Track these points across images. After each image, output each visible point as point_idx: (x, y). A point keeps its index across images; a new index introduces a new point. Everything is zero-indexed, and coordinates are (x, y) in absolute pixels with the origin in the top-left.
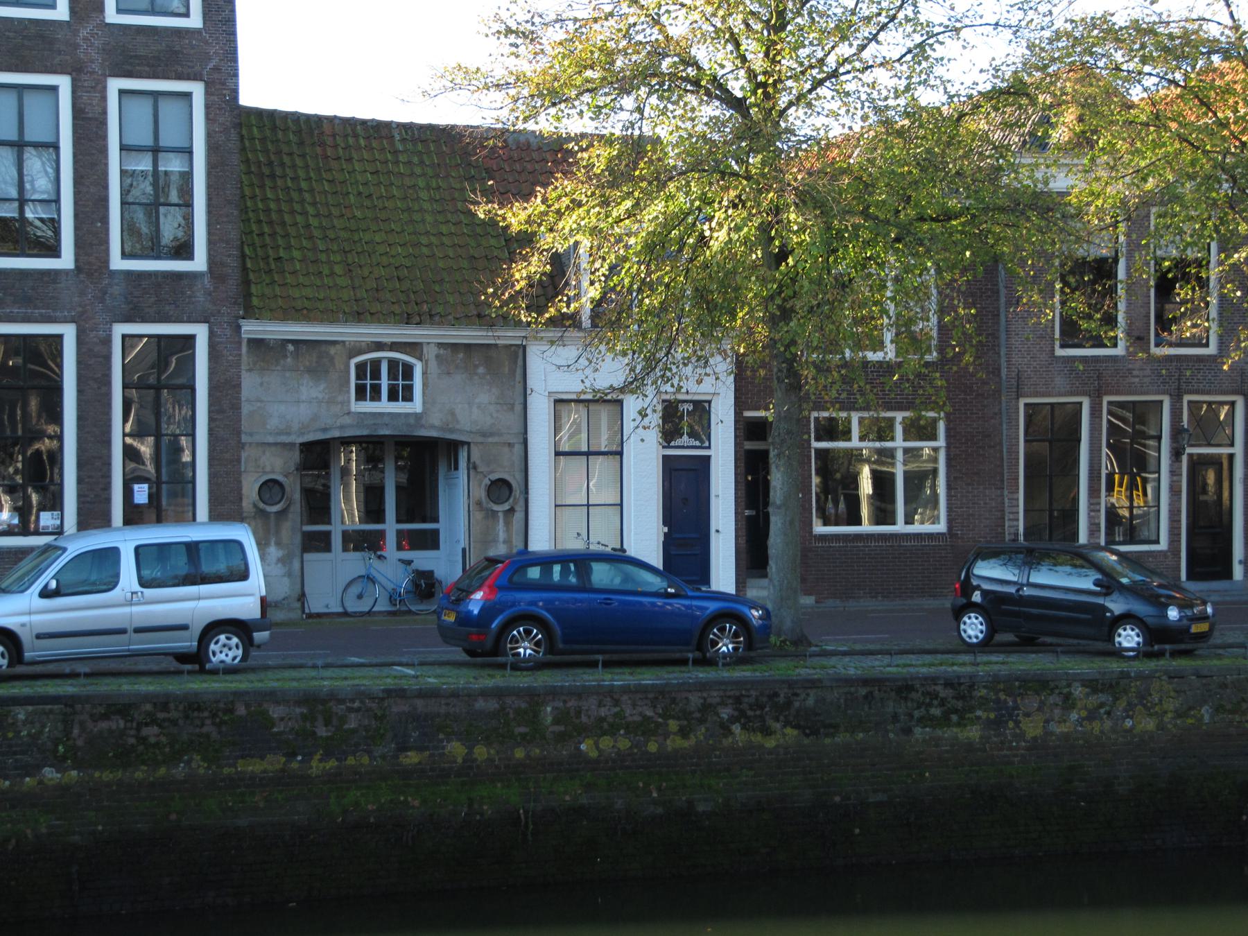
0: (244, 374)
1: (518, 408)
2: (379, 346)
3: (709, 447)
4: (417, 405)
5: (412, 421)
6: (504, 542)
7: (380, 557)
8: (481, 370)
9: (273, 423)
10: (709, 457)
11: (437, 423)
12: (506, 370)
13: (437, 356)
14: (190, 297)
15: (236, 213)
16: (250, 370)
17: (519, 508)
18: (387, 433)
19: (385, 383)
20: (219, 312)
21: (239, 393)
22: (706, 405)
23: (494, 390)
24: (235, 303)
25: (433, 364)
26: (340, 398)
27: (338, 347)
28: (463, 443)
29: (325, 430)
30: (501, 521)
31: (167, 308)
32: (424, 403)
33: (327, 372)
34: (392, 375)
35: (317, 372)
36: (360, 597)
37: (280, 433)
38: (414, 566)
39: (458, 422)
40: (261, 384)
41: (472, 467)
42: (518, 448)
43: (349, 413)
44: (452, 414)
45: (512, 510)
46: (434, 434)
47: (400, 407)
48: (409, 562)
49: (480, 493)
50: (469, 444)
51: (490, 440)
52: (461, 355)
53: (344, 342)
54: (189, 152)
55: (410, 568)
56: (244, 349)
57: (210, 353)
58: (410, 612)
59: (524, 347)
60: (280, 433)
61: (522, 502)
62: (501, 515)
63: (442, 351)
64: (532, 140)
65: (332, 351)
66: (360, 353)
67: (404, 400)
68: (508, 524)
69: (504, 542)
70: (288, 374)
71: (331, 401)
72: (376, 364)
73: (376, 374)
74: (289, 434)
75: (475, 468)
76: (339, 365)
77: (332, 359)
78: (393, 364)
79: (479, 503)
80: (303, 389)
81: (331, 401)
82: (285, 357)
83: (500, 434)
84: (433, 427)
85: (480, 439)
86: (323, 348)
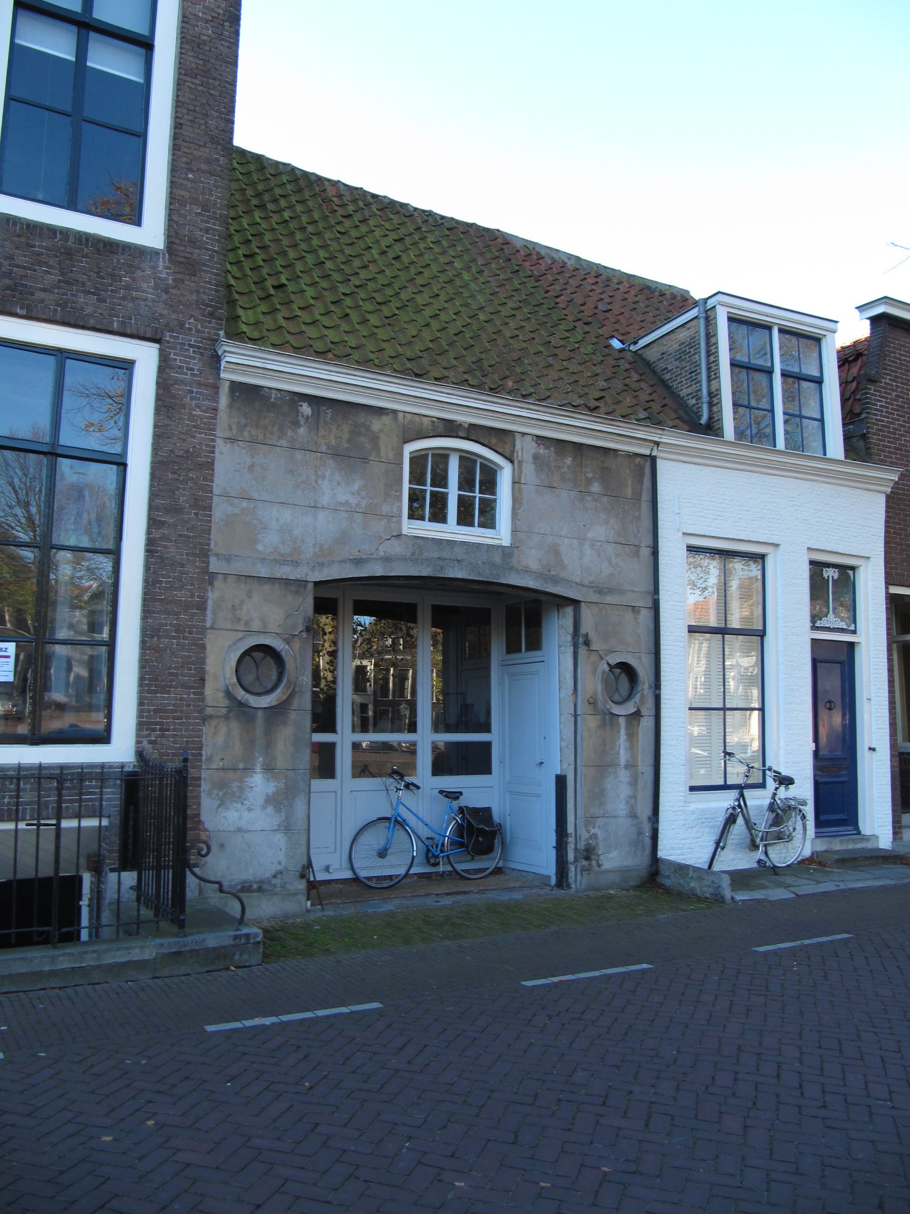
0: (221, 447)
1: (646, 552)
2: (450, 429)
3: (854, 632)
4: (502, 533)
5: (497, 559)
6: (626, 767)
7: (407, 786)
8: (596, 488)
9: (269, 541)
10: (851, 646)
11: (534, 565)
12: (629, 492)
13: (536, 457)
14: (128, 287)
15: (217, 197)
16: (232, 440)
17: (647, 710)
18: (460, 575)
19: (453, 492)
20: (182, 325)
21: (210, 478)
22: (851, 573)
23: (612, 521)
24: (211, 315)
25: (529, 469)
26: (385, 509)
27: (386, 419)
28: (562, 602)
29: (359, 562)
30: (623, 732)
31: (82, 299)
32: (514, 531)
33: (366, 460)
34: (466, 482)
35: (352, 457)
36: (382, 854)
37: (282, 561)
38: (463, 802)
39: (563, 566)
40: (251, 468)
41: (580, 641)
42: (645, 616)
43: (399, 536)
44: (555, 551)
45: (637, 715)
46: (531, 584)
47: (474, 534)
48: (454, 795)
49: (592, 684)
50: (575, 603)
51: (609, 599)
52: (569, 461)
53: (395, 412)
54: (145, 44)
55: (455, 805)
56: (224, 400)
57: (158, 398)
58: (456, 875)
59: (653, 460)
60: (282, 561)
61: (650, 703)
62: (622, 721)
63: (542, 451)
64: (570, 263)
65: (377, 424)
66: (422, 435)
67: (481, 525)
68: (631, 736)
69: (626, 767)
70: (299, 455)
71: (371, 512)
72: (442, 457)
73: (441, 479)
74: (296, 563)
75: (587, 643)
76: (386, 452)
77: (375, 439)
78: (467, 461)
79: (592, 702)
80: (325, 485)
81: (371, 512)
82: (296, 424)
83: (623, 592)
84: (527, 571)
85: (594, 598)
86: (361, 418)
